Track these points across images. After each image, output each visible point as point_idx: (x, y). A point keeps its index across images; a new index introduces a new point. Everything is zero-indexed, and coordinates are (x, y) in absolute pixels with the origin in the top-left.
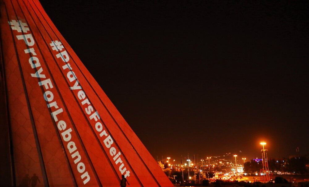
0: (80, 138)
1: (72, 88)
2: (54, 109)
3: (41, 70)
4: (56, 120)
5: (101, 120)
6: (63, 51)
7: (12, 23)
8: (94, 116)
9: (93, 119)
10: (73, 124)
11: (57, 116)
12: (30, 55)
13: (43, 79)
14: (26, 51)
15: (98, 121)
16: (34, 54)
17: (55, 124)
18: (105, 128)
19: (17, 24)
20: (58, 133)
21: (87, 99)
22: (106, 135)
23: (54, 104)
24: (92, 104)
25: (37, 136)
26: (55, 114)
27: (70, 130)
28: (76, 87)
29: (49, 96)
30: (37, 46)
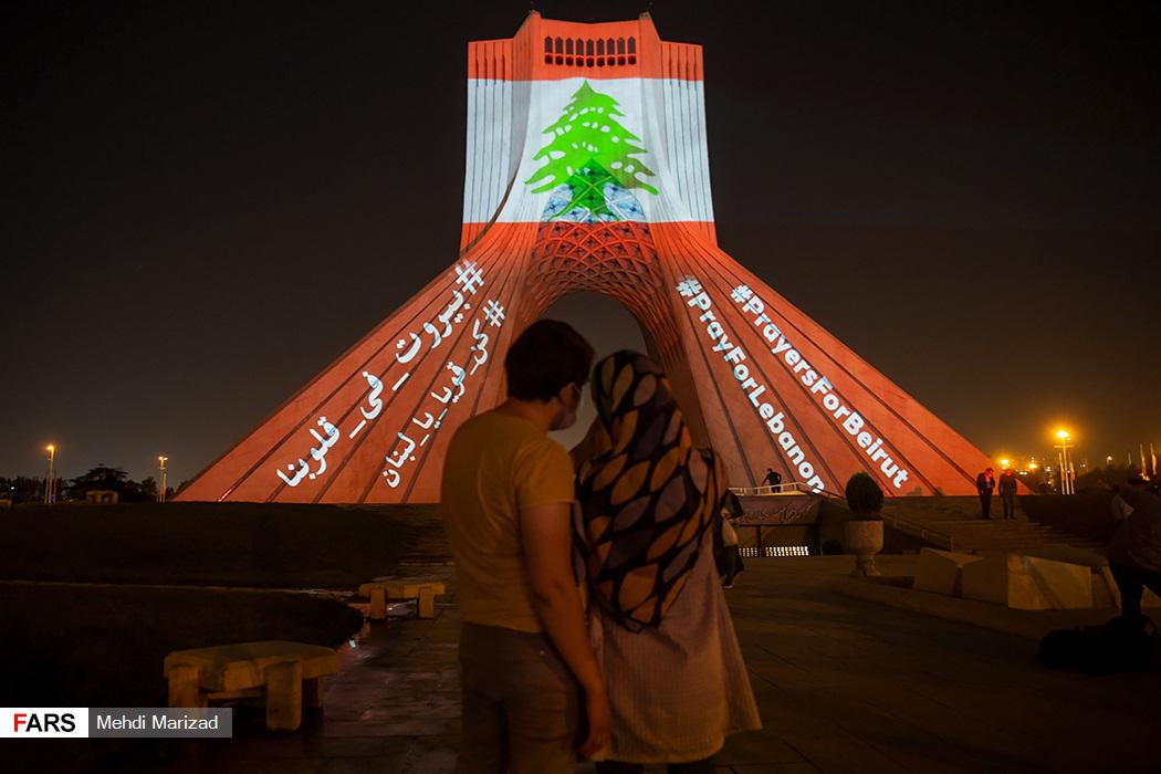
0: (796, 423)
1: (774, 351)
2: (751, 389)
3: (725, 338)
4: (756, 404)
5: (835, 391)
6: (752, 296)
7: (679, 288)
8: (821, 386)
9: (819, 392)
10: (783, 404)
11: (757, 398)
12: (709, 321)
13: (732, 349)
14: (703, 319)
15: (829, 392)
16: (713, 318)
17: (756, 410)
18: (845, 401)
19: (687, 285)
20: (763, 423)
21: (803, 361)
22: (847, 413)
23: (751, 382)
24: (813, 368)
25: (734, 432)
26: (753, 396)
27: (781, 415)
28: (781, 347)
29: (741, 372)
30: (715, 307)
